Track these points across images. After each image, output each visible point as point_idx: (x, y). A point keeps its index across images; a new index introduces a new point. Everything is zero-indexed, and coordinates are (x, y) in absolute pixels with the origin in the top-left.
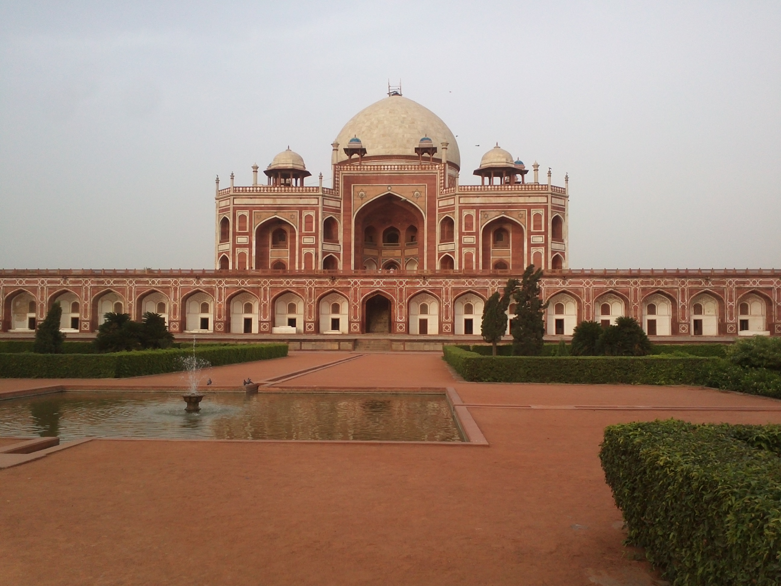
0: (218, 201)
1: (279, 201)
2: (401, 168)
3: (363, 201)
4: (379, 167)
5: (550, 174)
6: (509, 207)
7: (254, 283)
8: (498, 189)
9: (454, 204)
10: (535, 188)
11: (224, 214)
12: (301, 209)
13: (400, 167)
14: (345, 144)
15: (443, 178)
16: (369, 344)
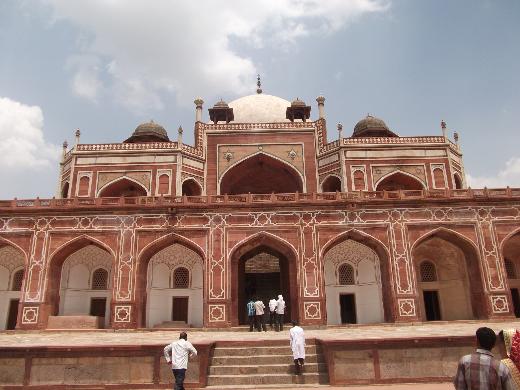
0: (63, 166)
1: (130, 160)
2: (273, 127)
3: (231, 163)
4: (248, 126)
5: (443, 125)
6: (404, 161)
7: (21, 225)
8: (388, 141)
9: (339, 160)
10: (430, 140)
11: (66, 179)
12: (155, 168)
13: (272, 125)
14: (209, 104)
15: (321, 135)
16: (256, 361)
